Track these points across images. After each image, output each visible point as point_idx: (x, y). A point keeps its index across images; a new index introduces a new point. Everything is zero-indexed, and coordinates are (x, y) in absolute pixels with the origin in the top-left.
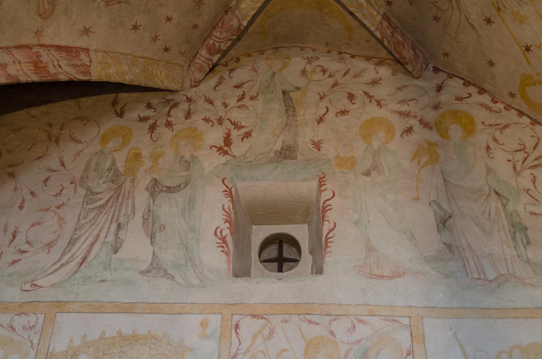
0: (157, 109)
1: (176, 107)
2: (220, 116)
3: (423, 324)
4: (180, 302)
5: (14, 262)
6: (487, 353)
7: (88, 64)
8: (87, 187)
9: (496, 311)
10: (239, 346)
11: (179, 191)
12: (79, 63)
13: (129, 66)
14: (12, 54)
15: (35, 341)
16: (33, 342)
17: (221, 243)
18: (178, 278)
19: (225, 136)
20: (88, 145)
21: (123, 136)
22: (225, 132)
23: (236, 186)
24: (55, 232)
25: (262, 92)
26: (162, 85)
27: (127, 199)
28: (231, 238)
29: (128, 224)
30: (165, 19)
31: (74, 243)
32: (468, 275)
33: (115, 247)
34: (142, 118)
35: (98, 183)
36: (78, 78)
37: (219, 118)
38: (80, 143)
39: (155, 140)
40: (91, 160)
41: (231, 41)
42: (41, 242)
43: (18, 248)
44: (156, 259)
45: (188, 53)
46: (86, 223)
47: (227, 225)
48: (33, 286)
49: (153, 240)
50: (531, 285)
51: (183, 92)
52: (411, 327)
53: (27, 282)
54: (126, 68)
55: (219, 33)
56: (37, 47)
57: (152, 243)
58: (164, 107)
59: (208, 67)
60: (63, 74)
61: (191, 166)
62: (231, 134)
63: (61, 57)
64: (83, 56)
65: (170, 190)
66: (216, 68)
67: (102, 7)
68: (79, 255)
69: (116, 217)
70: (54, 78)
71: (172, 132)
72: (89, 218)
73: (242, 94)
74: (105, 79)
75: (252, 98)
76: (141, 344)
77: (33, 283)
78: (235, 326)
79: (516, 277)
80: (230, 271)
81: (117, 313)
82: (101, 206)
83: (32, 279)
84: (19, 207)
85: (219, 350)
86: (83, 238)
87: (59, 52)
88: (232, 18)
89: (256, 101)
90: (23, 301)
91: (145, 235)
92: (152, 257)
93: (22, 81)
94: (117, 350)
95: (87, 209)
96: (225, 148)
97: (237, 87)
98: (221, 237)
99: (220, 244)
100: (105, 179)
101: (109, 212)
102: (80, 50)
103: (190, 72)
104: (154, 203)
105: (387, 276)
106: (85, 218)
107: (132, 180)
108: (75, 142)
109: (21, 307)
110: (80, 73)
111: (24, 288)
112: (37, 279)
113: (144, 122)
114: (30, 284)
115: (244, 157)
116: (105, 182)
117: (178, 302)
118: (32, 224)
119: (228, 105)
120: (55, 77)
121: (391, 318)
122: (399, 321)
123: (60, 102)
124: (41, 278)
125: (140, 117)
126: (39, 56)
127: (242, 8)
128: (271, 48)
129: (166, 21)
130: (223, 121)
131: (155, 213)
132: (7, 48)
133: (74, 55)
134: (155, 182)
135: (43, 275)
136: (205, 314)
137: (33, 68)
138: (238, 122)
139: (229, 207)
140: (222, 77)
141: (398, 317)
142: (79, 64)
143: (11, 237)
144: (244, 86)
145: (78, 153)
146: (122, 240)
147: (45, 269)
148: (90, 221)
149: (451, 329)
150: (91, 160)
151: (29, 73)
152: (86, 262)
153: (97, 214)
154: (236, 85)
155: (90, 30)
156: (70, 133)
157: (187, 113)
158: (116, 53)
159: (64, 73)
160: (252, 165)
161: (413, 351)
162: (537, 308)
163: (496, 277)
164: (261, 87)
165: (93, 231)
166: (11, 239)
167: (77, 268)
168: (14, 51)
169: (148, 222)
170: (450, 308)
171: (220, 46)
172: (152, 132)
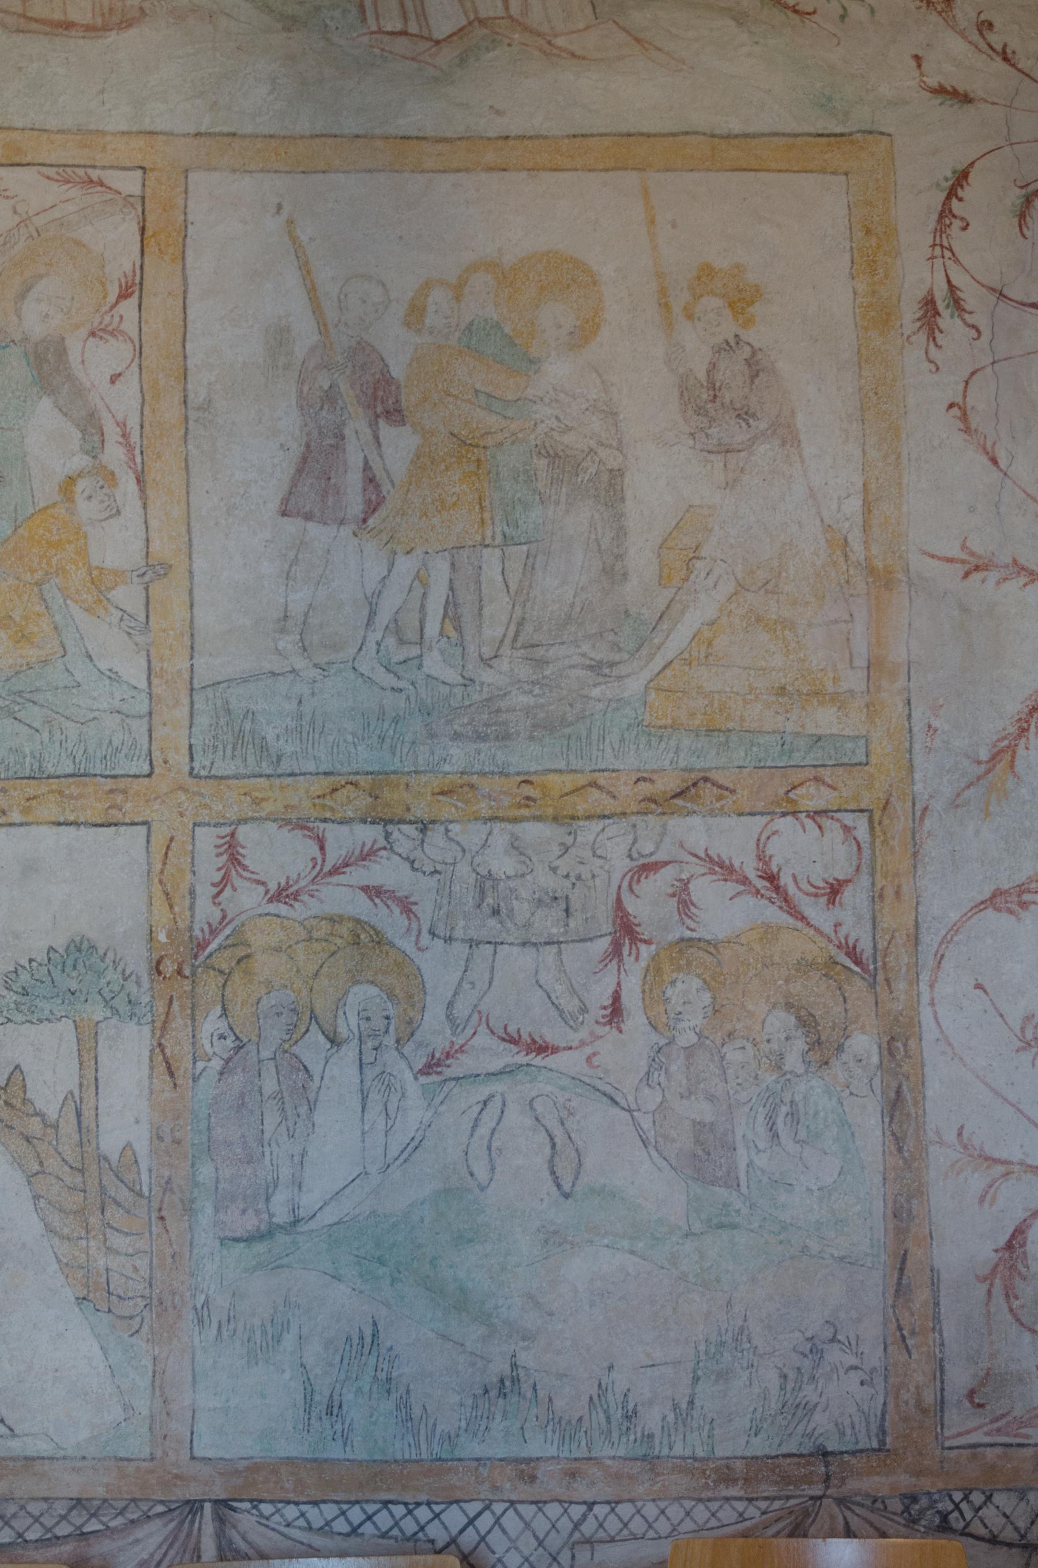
3: (186, 192)
6: (383, 285)
9: (439, 147)
32: (364, 20)
50: (573, 55)
52: (143, 205)
79: (527, 29)
105: (82, 26)
121: (81, 172)
122: (106, 182)
141: (104, 168)
149: (279, 207)
161: (141, 284)
162: (574, 136)
163: (461, 30)
170: (284, 137)
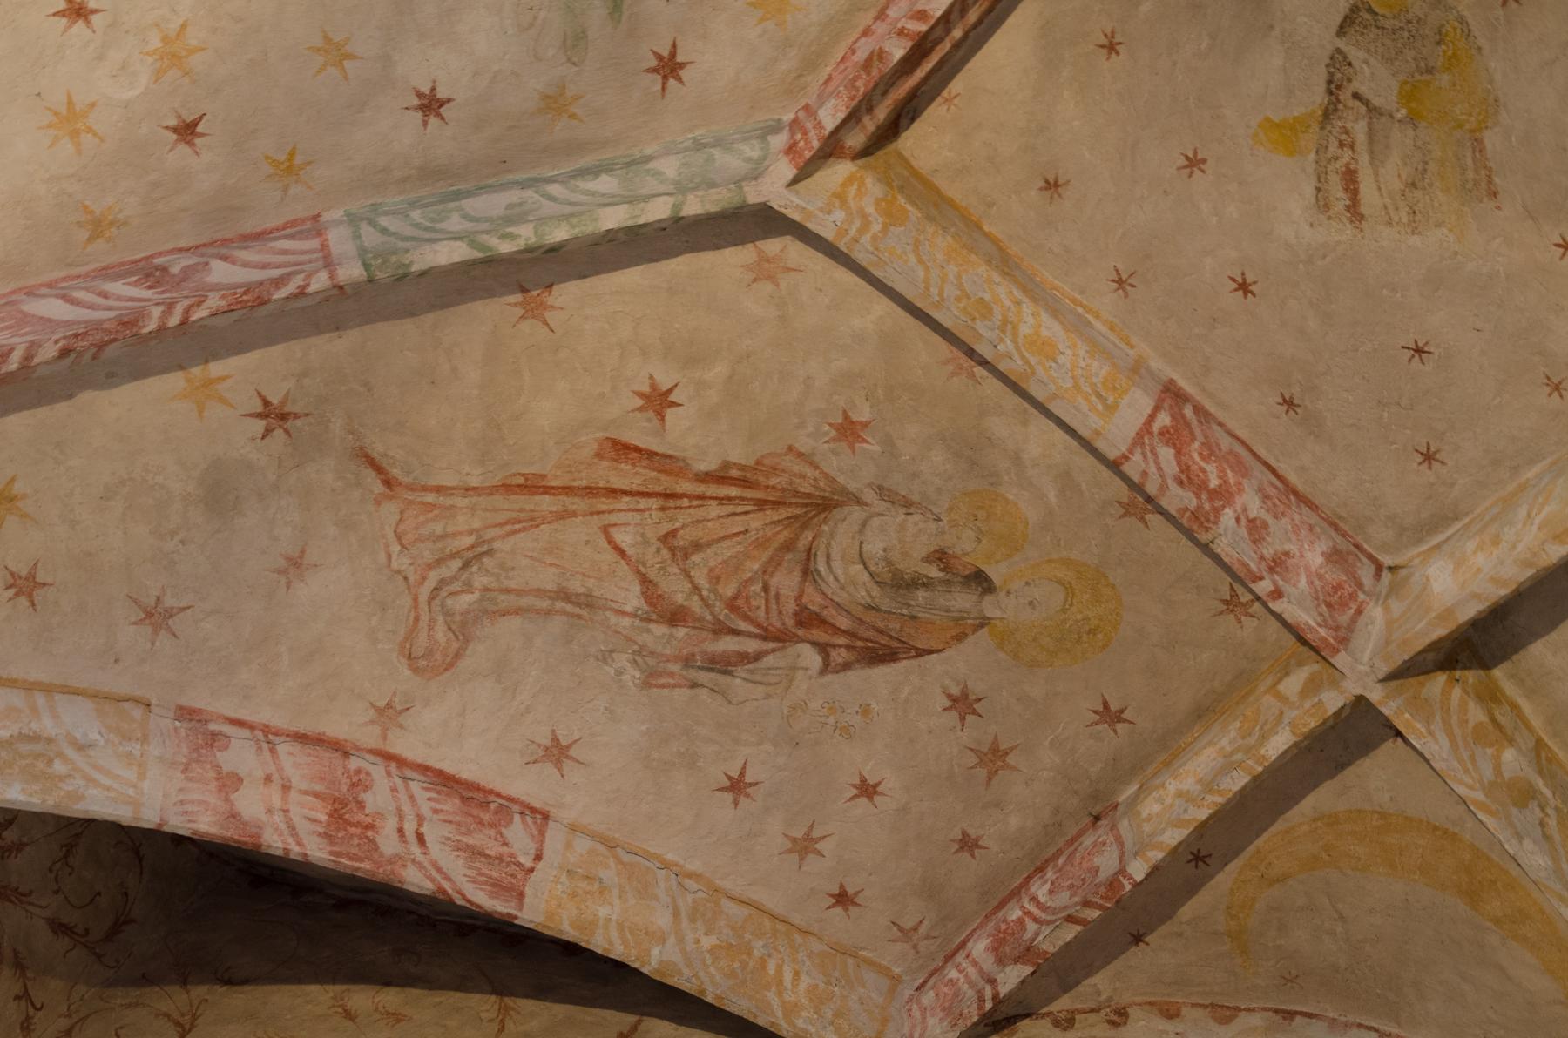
7: (527, 861)
12: (493, 849)
13: (676, 914)
14: (273, 751)
26: (783, 1023)
30: (854, 786)
36: (474, 899)
41: (1079, 928)
45: (927, 937)
54: (663, 919)
55: (1047, 886)
56: (371, 758)
59: (975, 1006)
60: (420, 866)
63: (436, 811)
64: (519, 835)
67: (631, 684)
70: (381, 870)
74: (567, 930)
87: (438, 793)
88: (1104, 844)
93: (270, 846)
102: (516, 808)
110: (485, 883)
120: (389, 868)
123: (452, 993)
126: (360, 783)
127: (1144, 814)
128: (1265, 1009)
129: (855, 791)
132: (267, 730)
133: (486, 817)
137: (324, 818)
142: (492, 853)
151: (303, 827)
155: (572, 752)
158: (647, 856)
159: (426, 864)
168: (284, 748)
171: (1037, 934)
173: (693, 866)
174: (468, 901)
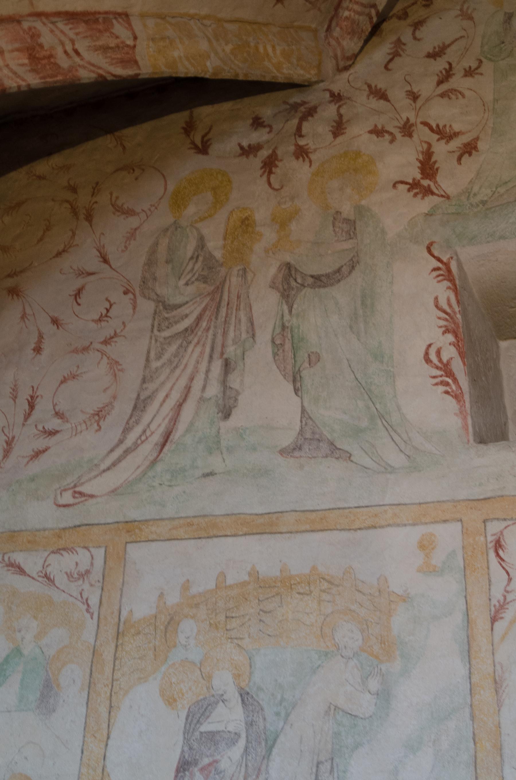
0: (274, 126)
1: (312, 116)
2: (405, 119)
4: (369, 504)
5: (37, 454)
7: (130, 42)
8: (155, 297)
10: (508, 584)
11: (339, 281)
12: (112, 43)
13: (209, 41)
15: (94, 601)
16: (89, 602)
17: (441, 376)
18: (358, 455)
19: (421, 158)
20: (147, 217)
21: (214, 189)
22: (420, 149)
23: (457, 255)
24: (105, 390)
25: (488, 56)
26: (278, 74)
27: (236, 310)
28: (461, 364)
29: (244, 359)
31: (144, 407)
33: (225, 405)
34: (247, 148)
35: (177, 287)
37: (402, 123)
38: (132, 215)
39: (277, 186)
40: (156, 244)
42: (82, 412)
43: (40, 428)
44: (310, 422)
46: (162, 366)
47: (450, 338)
48: (76, 495)
49: (298, 385)
51: (321, 85)
53: (65, 490)
54: (204, 46)
56: (31, 19)
57: (296, 391)
58: (288, 120)
59: (368, 23)
60: (84, 67)
61: (357, 229)
62: (433, 152)
65: (321, 281)
66: (385, 26)
68: (156, 430)
69: (218, 349)
70: (68, 77)
71: (310, 166)
72: (166, 356)
73: (445, 69)
74: (165, 71)
75: (469, 73)
76: (299, 593)
77: (77, 489)
78: (493, 544)
80: (468, 433)
81: (245, 534)
82: (186, 330)
83: (73, 482)
84: (34, 350)
85: (466, 597)
86: (161, 396)
87: (72, 24)
89: (476, 76)
90: (62, 526)
91: (281, 377)
92: (301, 418)
93: (10, 88)
94: (252, 608)
95: (161, 340)
96: (425, 183)
97: (433, 55)
98: (439, 365)
99: (440, 379)
100: (188, 277)
101: (204, 339)
103: (331, 40)
104: (290, 311)
106: (159, 357)
107: (241, 272)
108: (123, 213)
109: (59, 537)
111: (62, 501)
112: (82, 481)
113: (251, 156)
114: (70, 492)
115: (467, 194)
116: (190, 282)
117: (366, 505)
118: (61, 378)
119: (420, 95)
120: (71, 74)
124: (90, 480)
125: (242, 148)
126: (35, 35)
130: (414, 128)
131: (296, 330)
133: (101, 27)
134: (287, 271)
135: (94, 474)
136: (426, 523)
137: (26, 61)
138: (445, 126)
139: (448, 300)
140: (399, 40)
142: (112, 45)
143: (27, 407)
144: (448, 51)
145: (132, 234)
146: (237, 391)
147: (96, 462)
148: (170, 361)
150: (156, 244)
151: (20, 71)
152: (172, 441)
153: (181, 346)
154: (431, 51)
156: (111, 199)
157: (335, 124)
158: (182, 16)
159: (86, 65)
160: (487, 209)
164: (486, 48)
165: (177, 380)
166: (27, 411)
167: (155, 455)
169: (283, 351)
172: (270, 172)
173: (204, 11)
174: (114, 76)
